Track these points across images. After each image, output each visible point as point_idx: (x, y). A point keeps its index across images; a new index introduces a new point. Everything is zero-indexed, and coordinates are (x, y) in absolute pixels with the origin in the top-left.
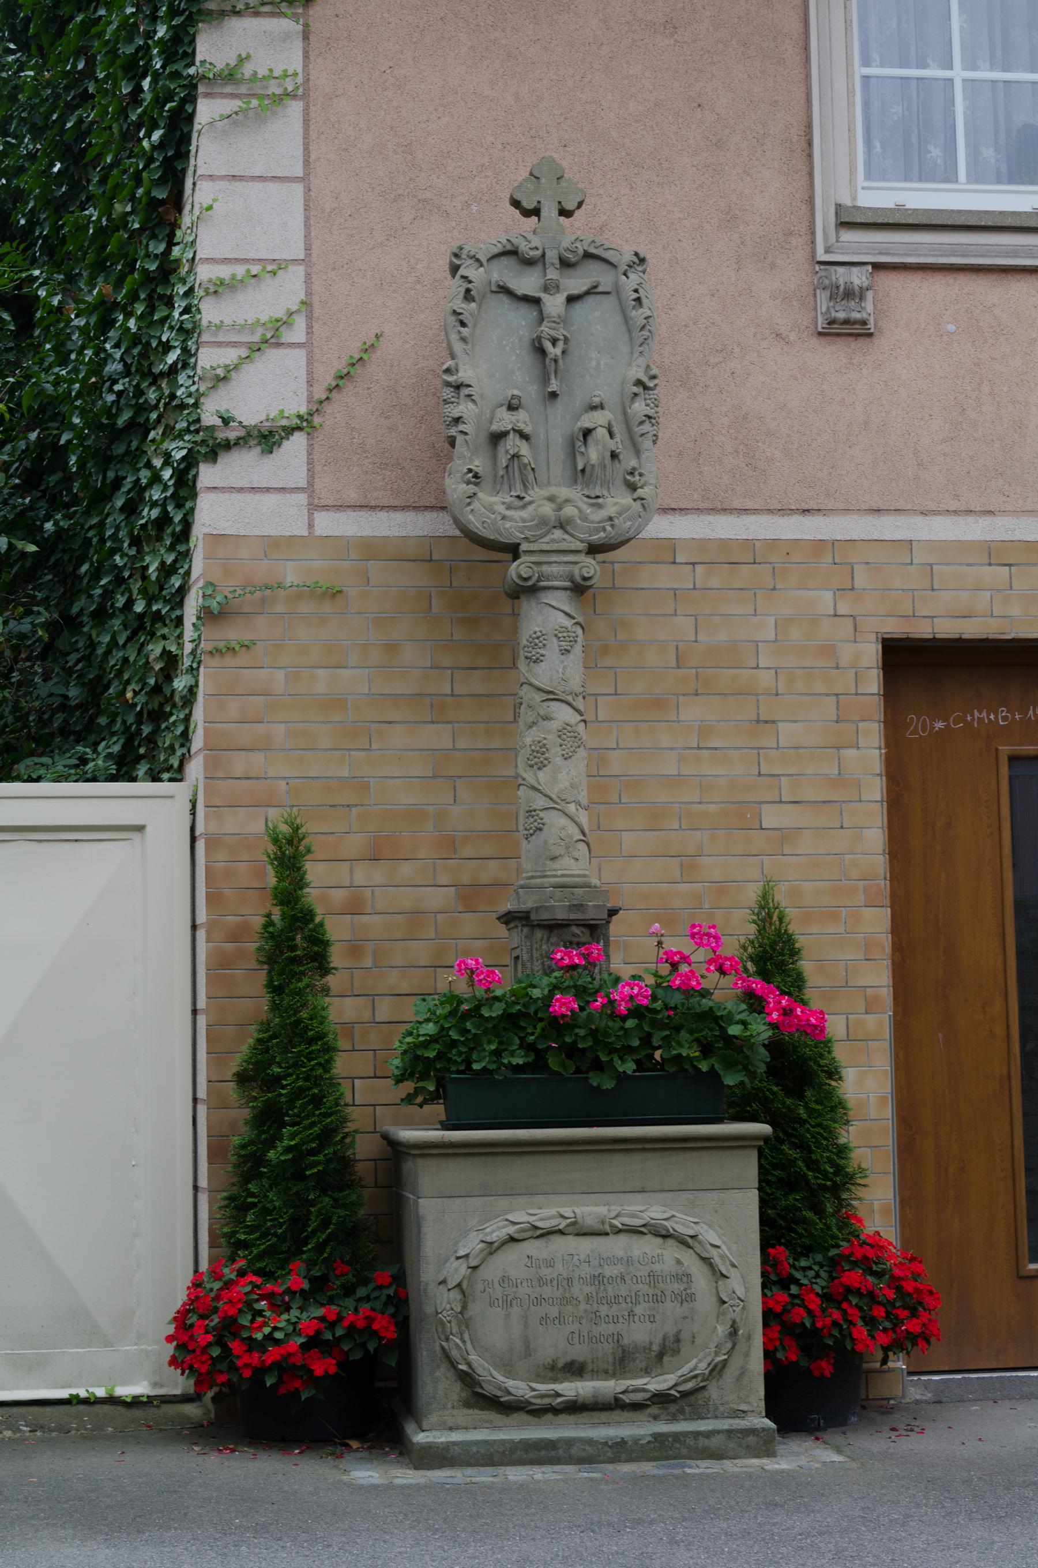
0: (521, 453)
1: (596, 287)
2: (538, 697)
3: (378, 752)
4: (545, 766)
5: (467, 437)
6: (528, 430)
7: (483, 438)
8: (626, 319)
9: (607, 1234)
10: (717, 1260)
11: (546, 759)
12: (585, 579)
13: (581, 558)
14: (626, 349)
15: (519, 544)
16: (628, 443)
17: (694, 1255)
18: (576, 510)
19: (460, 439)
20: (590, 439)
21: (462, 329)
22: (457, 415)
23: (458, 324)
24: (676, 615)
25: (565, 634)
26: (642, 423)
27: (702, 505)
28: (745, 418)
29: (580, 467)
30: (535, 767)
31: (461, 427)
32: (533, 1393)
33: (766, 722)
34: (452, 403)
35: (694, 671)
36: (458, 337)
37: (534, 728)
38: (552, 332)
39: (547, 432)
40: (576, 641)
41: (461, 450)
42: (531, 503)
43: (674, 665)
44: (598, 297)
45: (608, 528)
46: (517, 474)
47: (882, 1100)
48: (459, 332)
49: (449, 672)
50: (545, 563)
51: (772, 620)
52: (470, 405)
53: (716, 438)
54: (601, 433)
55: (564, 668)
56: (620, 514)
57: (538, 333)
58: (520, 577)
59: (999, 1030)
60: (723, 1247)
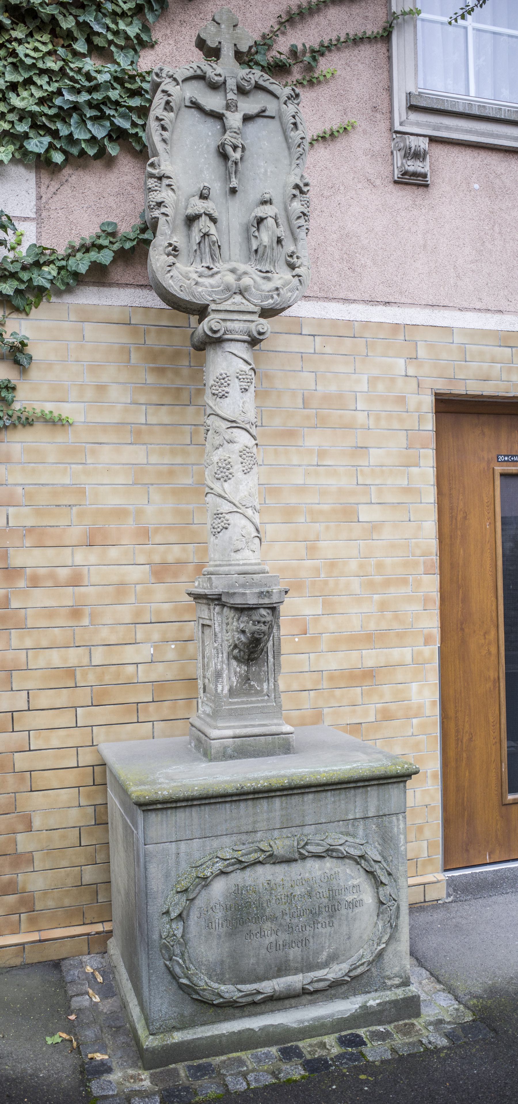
0: (211, 232)
1: (264, 111)
2: (225, 425)
3: (91, 466)
4: (230, 479)
5: (168, 218)
6: (216, 215)
7: (180, 221)
8: (286, 138)
9: (295, 860)
10: (379, 872)
11: (230, 474)
12: (260, 334)
13: (255, 317)
14: (286, 162)
15: (208, 305)
16: (288, 233)
17: (361, 870)
18: (252, 280)
19: (162, 220)
20: (262, 227)
21: (163, 133)
22: (160, 200)
23: (160, 128)
24: (303, 371)
25: (244, 377)
26: (299, 218)
27: (319, 295)
28: (347, 236)
29: (254, 247)
30: (222, 480)
31: (163, 210)
32: (241, 994)
33: (362, 448)
34: (156, 191)
35: (314, 411)
36: (160, 139)
37: (221, 449)
38: (233, 140)
39: (228, 219)
40: (252, 383)
41: (163, 228)
42: (217, 273)
43: (302, 406)
44: (265, 120)
45: (275, 296)
46: (207, 250)
47: (434, 702)
48: (161, 135)
49: (144, 407)
50: (229, 320)
51: (365, 378)
52: (170, 193)
53: (329, 249)
54: (270, 221)
55: (243, 403)
56: (284, 286)
57: (223, 141)
58: (211, 330)
59: (493, 650)
60: (383, 862)
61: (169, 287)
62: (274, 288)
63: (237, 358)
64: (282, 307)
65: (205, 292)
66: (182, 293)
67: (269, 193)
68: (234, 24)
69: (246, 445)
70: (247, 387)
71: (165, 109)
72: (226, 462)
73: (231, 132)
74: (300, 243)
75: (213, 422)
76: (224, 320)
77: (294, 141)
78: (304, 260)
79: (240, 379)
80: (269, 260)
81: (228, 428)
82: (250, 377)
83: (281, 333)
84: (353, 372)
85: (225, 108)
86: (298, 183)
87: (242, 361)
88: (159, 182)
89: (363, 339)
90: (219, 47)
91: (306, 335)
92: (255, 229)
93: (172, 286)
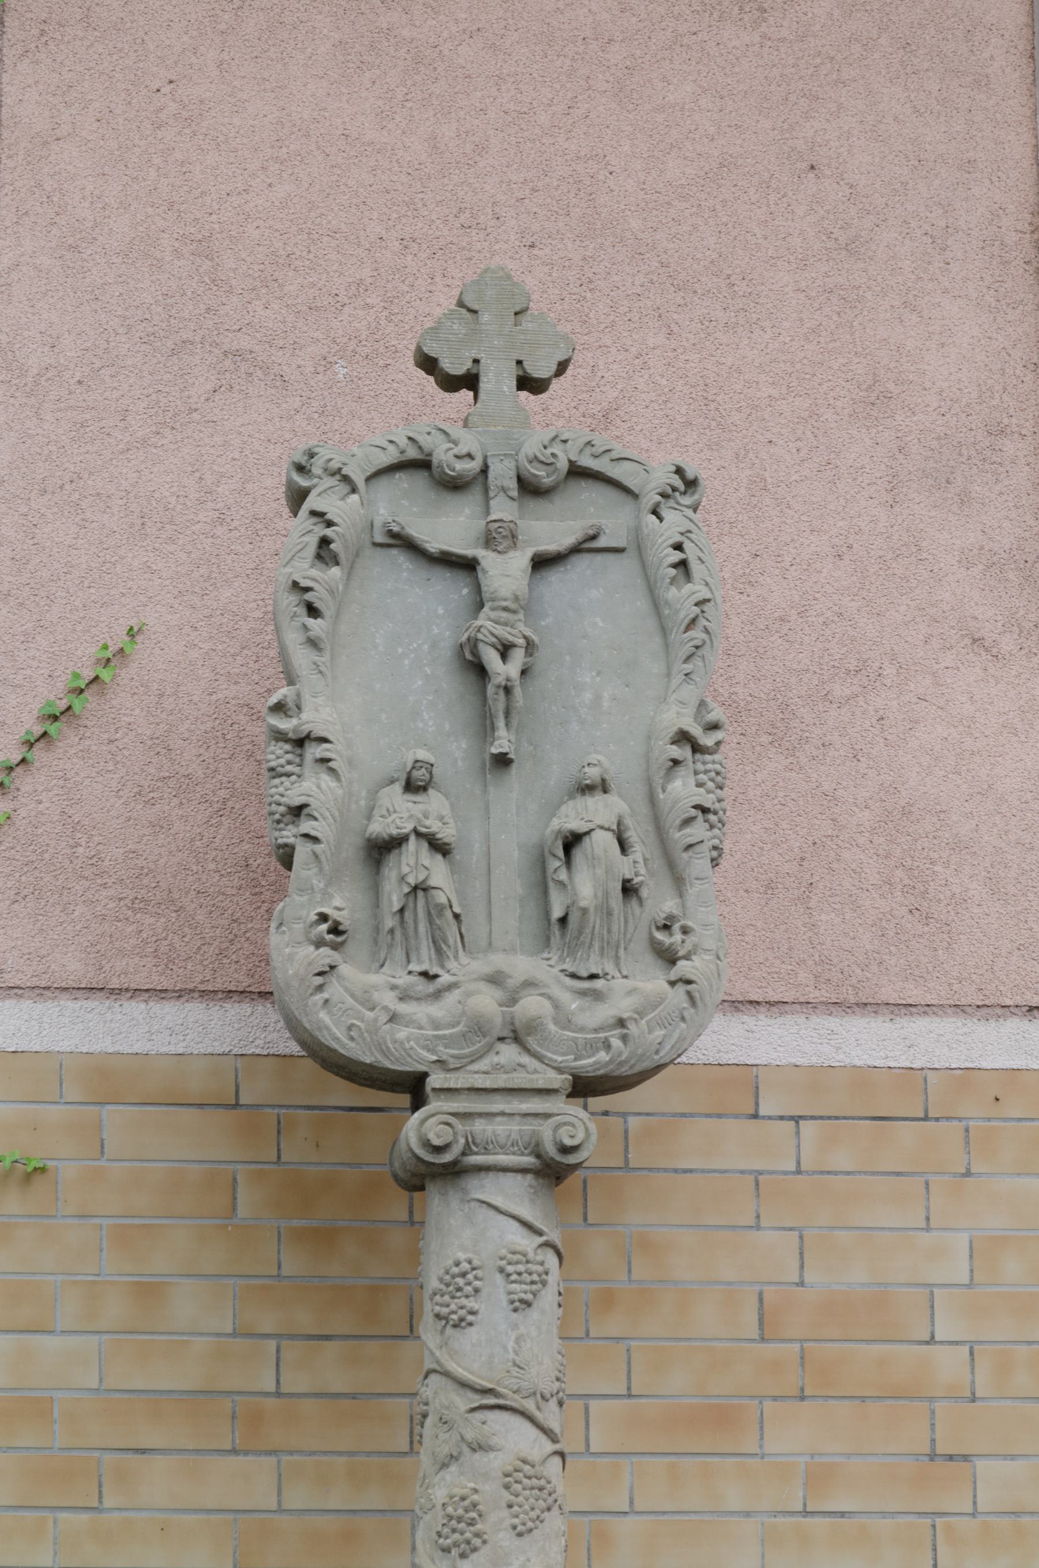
0: (432, 883)
1: (594, 538)
2: (463, 1401)
3: (116, 1515)
4: (475, 1550)
5: (318, 848)
6: (446, 833)
7: (351, 850)
8: (657, 605)
11: (477, 1535)
12: (566, 1150)
13: (558, 1105)
14: (657, 668)
15: (423, 1076)
16: (658, 863)
18: (547, 1003)
19: (302, 852)
20: (578, 854)
21: (311, 622)
22: (297, 801)
23: (302, 611)
24: (758, 1228)
25: (521, 1268)
26: (688, 821)
27: (814, 995)
28: (907, 812)
29: (557, 913)
30: (454, 1552)
31: (306, 826)
33: (951, 1458)
34: (288, 775)
35: (796, 1347)
36: (301, 637)
37: (453, 1468)
38: (499, 630)
39: (487, 837)
40: (544, 1283)
41: (305, 874)
42: (451, 987)
43: (755, 1334)
44: (599, 558)
45: (616, 1043)
46: (423, 927)
48: (305, 628)
49: (272, 1344)
50: (480, 1115)
51: (962, 1240)
52: (326, 780)
53: (846, 855)
54: (603, 842)
55: (518, 1340)
56: (641, 1013)
57: (471, 632)
58: (427, 1144)
61: (320, 1029)
62: (612, 1021)
63: (501, 1217)
64: (638, 1069)
65: (417, 1040)
66: (352, 1045)
67: (599, 764)
68: (518, 309)
69: (523, 1455)
70: (529, 1297)
71: (319, 557)
72: (467, 1503)
73: (493, 609)
74: (692, 891)
75: (435, 1390)
76: (465, 1116)
77: (677, 611)
78: (705, 937)
79: (509, 1275)
80: (596, 945)
81: (473, 1410)
82: (540, 1269)
83: (692, 1115)
84: (923, 1225)
85: (482, 541)
86: (686, 728)
87: (515, 1225)
88: (299, 751)
89: (955, 1123)
90: (474, 371)
91: (770, 1118)
92: (557, 864)
93: (328, 1028)
